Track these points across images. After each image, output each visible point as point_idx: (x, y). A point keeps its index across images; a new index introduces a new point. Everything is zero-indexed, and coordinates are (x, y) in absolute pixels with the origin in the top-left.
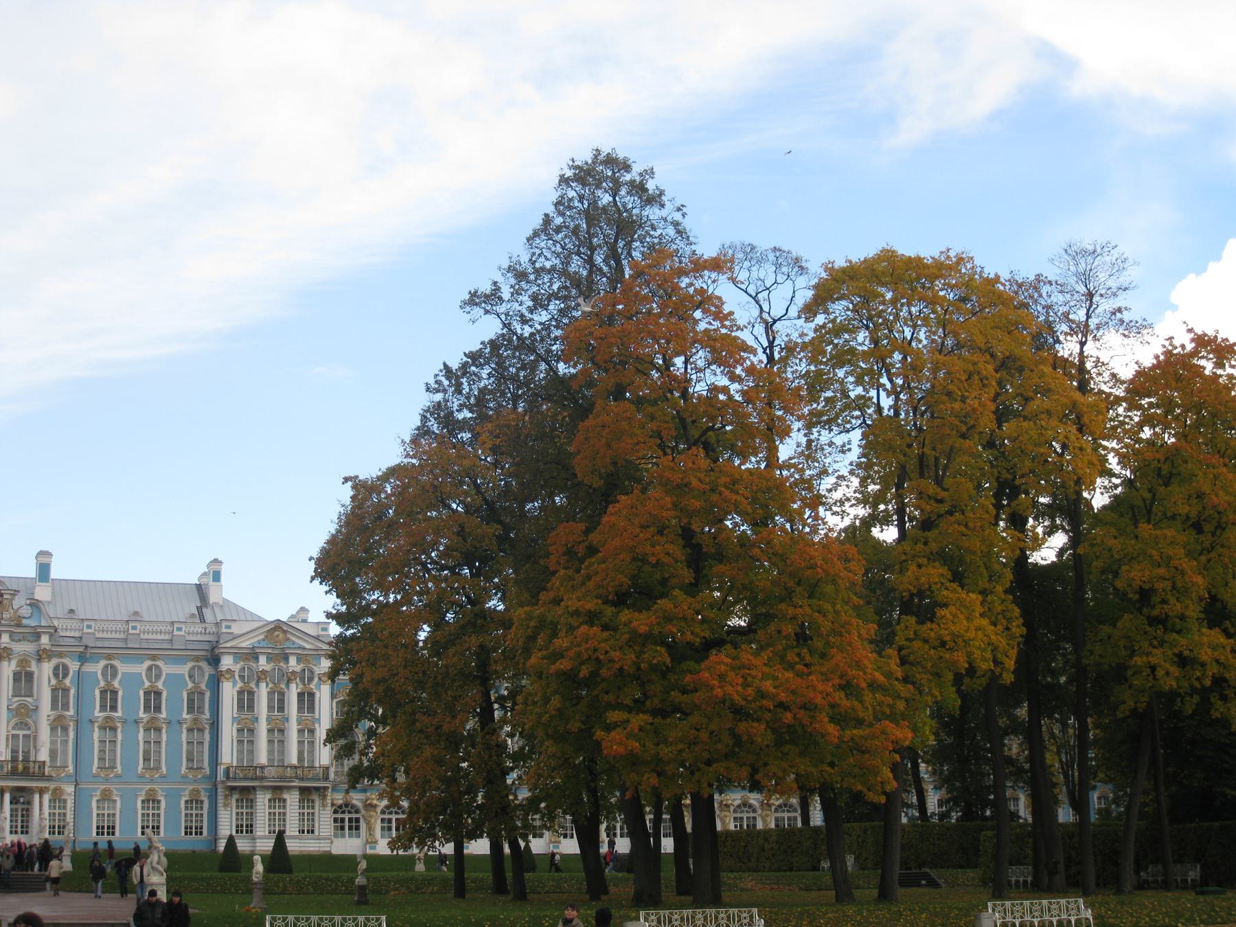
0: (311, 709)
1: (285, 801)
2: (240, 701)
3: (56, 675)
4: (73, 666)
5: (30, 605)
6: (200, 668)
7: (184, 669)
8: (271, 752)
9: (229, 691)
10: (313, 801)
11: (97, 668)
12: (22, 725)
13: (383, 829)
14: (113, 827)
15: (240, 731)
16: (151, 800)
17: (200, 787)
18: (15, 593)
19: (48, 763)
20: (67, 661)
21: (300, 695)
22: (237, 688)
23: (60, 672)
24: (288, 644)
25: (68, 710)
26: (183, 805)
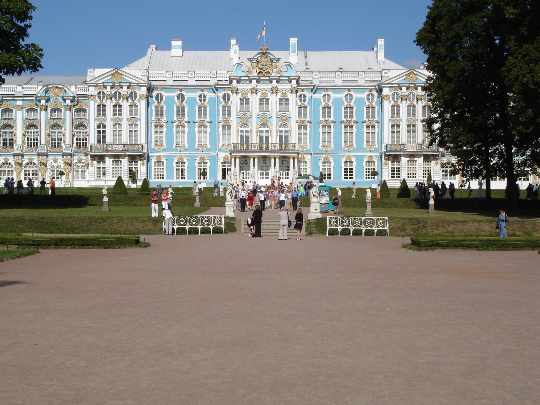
2: (393, 111)
3: (301, 100)
4: (308, 95)
5: (286, 65)
6: (372, 95)
7: (364, 95)
8: (409, 137)
11: (319, 95)
12: (284, 125)
14: (330, 175)
15: (393, 126)
16: (348, 161)
19: (297, 144)
23: (302, 98)
24: (417, 81)
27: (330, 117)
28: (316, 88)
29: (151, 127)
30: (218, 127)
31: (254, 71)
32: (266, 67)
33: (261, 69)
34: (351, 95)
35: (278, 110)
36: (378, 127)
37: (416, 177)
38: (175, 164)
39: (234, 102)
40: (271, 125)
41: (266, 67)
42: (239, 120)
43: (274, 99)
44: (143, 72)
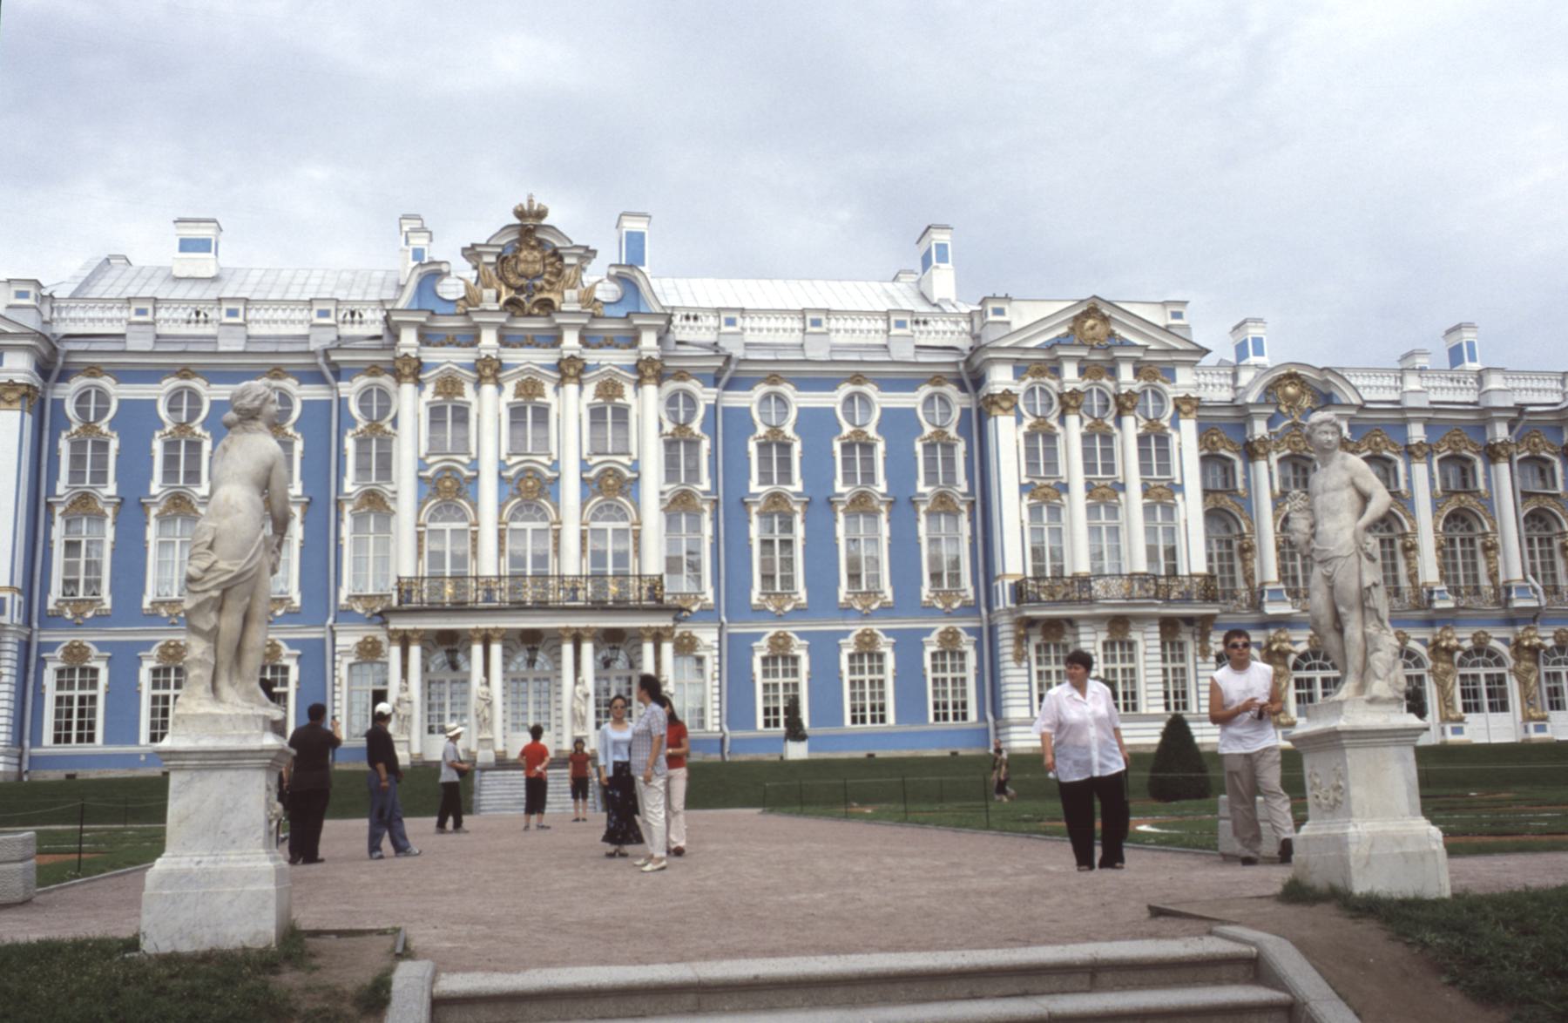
0: (1165, 468)
1: (1131, 645)
2: (1031, 453)
3: (674, 416)
4: (706, 396)
6: (944, 399)
7: (912, 400)
9: (1008, 434)
10: (1181, 645)
11: (747, 400)
13: (1299, 698)
15: (1034, 511)
17: (959, 625)
18: (588, 254)
20: (693, 386)
21: (1143, 440)
22: (1025, 428)
25: (698, 481)
26: (928, 662)
27: (789, 482)
28: (733, 367)
29: (50, 522)
30: (339, 520)
31: (489, 294)
32: (538, 283)
33: (519, 290)
34: (864, 398)
35: (586, 449)
36: (972, 520)
37: (1134, 707)
38: (145, 676)
39: (406, 423)
40: (557, 508)
41: (538, 283)
42: (428, 489)
43: (570, 406)
44: (20, 295)
